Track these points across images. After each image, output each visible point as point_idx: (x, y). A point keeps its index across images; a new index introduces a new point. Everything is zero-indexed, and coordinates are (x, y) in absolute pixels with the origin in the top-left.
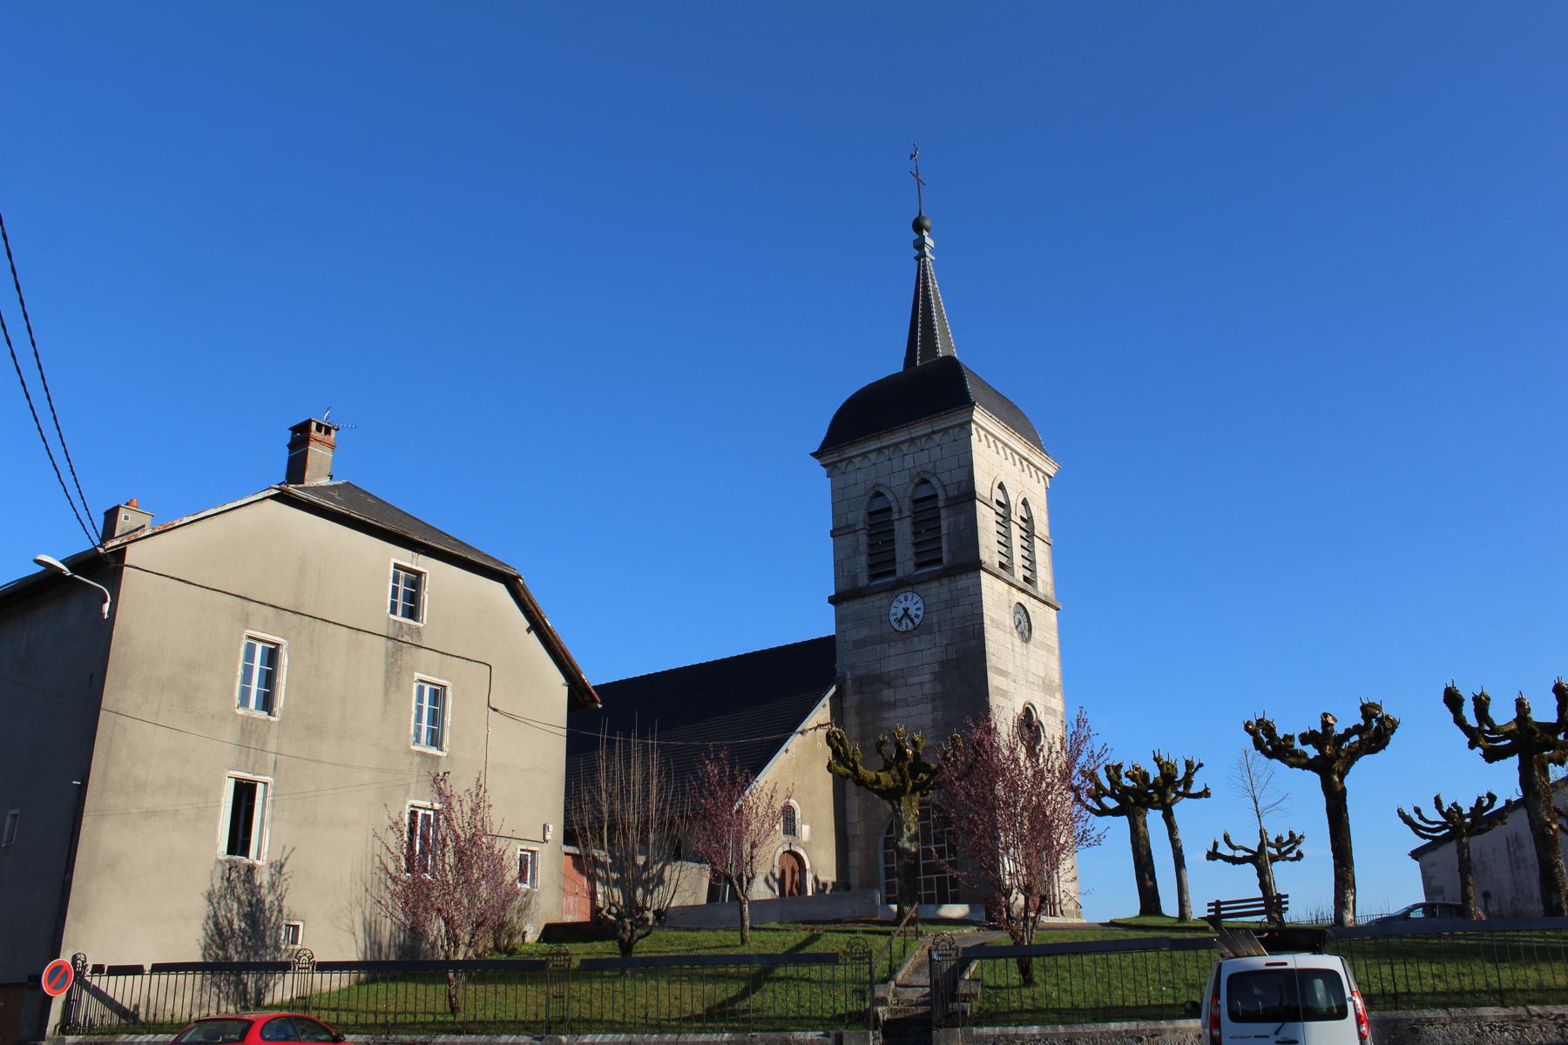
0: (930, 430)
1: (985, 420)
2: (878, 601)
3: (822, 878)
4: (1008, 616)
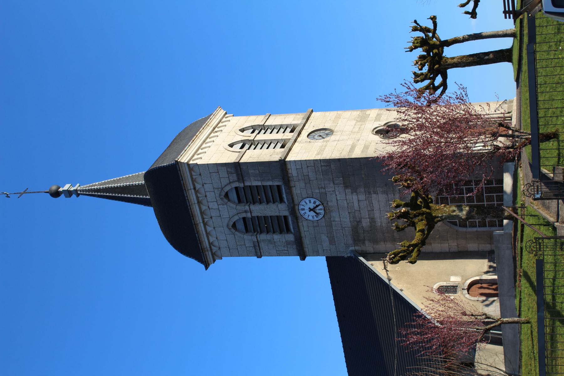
0: (193, 191)
2: (304, 228)
3: (486, 269)
4: (316, 144)
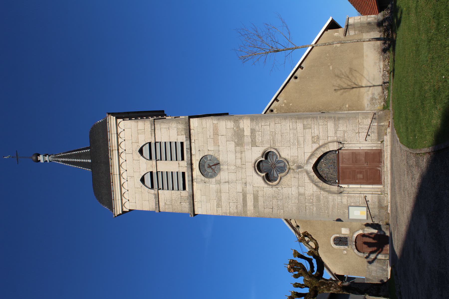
1: (117, 201)
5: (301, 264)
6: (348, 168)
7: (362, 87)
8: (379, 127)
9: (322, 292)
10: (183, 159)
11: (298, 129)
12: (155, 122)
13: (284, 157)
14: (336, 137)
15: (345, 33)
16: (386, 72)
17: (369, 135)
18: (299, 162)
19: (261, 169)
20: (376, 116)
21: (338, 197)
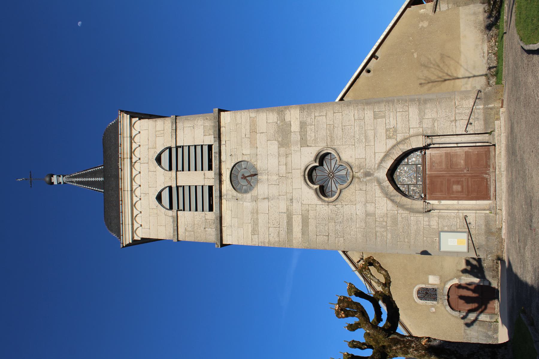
1: (127, 226)
5: (358, 304)
6: (439, 176)
7: (458, 78)
8: (486, 111)
9: (394, 355)
10: (210, 168)
11: (366, 118)
12: (177, 120)
13: (346, 160)
14: (422, 128)
15: (435, 7)
16: (492, 55)
17: (471, 124)
18: (367, 167)
19: (314, 181)
20: (482, 95)
21: (424, 218)
